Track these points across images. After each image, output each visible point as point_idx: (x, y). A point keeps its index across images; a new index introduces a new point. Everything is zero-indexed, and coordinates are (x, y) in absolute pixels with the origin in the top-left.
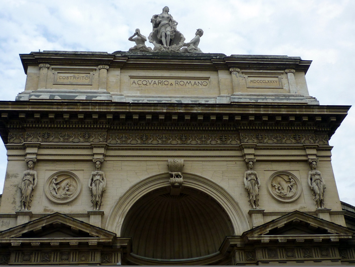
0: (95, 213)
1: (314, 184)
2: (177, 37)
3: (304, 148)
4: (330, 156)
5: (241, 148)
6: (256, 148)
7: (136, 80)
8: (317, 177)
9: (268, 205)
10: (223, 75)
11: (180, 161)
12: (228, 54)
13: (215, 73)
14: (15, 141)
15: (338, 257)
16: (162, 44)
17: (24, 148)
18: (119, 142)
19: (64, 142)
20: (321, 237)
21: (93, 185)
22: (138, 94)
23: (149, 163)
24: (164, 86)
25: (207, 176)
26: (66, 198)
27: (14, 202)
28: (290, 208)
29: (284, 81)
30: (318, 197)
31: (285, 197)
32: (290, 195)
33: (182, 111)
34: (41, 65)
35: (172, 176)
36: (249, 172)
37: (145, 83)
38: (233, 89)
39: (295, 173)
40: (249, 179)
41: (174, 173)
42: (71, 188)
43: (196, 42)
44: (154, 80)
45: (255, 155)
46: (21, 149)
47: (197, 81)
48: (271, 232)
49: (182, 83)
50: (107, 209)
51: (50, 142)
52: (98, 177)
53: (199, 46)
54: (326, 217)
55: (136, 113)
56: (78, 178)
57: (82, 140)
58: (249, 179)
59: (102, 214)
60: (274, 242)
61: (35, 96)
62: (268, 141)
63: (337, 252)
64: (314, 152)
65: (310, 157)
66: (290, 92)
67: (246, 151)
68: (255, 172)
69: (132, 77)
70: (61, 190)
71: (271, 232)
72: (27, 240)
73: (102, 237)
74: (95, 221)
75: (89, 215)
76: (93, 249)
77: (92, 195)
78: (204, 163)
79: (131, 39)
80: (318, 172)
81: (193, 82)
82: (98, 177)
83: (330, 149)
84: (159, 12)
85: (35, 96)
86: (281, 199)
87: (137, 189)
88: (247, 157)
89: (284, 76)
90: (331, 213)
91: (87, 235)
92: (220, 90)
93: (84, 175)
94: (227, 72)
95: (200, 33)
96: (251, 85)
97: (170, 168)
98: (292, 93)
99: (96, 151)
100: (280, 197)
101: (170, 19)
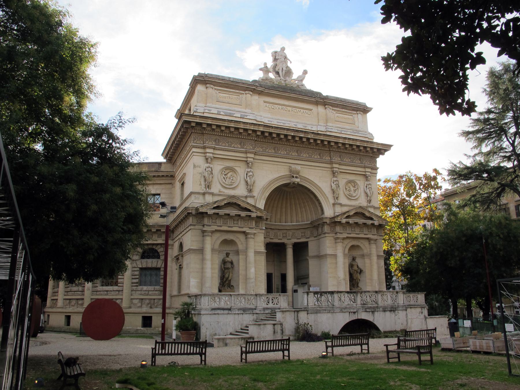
0: (251, 197)
1: (368, 190)
2: (289, 72)
3: (365, 167)
4: (376, 174)
5: (331, 163)
7: (268, 104)
8: (370, 186)
9: (343, 200)
10: (321, 109)
11: (298, 168)
12: (324, 94)
13: (316, 106)
14: (198, 142)
15: (376, 233)
16: (279, 76)
17: (204, 148)
18: (261, 150)
19: (228, 147)
20: (370, 222)
21: (248, 178)
23: (279, 167)
25: (311, 178)
26: (232, 185)
27: (200, 185)
29: (356, 119)
30: (369, 198)
31: (351, 196)
32: (354, 195)
33: (302, 136)
34: (208, 85)
35: (293, 177)
37: (273, 107)
38: (327, 122)
40: (335, 183)
41: (295, 175)
42: (234, 178)
43: (301, 79)
44: (278, 106)
45: (339, 169)
46: (201, 148)
47: (304, 111)
49: (295, 111)
50: (255, 194)
51: (220, 146)
53: (304, 82)
54: (372, 210)
55: (275, 133)
56: (238, 172)
57: (239, 146)
58: (335, 183)
59: (254, 197)
60: (348, 223)
61: (208, 110)
62: (347, 160)
63: (375, 230)
65: (367, 173)
66: (358, 128)
69: (265, 102)
70: (228, 179)
72: (216, 211)
73: (258, 213)
75: (246, 197)
76: (253, 219)
78: (310, 170)
79: (261, 69)
81: (302, 110)
83: (376, 169)
84: (279, 50)
85: (208, 110)
86: (349, 197)
87: (273, 183)
89: (356, 116)
90: (375, 208)
91: (249, 211)
92: (318, 120)
93: (241, 170)
94: (323, 107)
95: (305, 72)
99: (249, 155)
101: (286, 58)
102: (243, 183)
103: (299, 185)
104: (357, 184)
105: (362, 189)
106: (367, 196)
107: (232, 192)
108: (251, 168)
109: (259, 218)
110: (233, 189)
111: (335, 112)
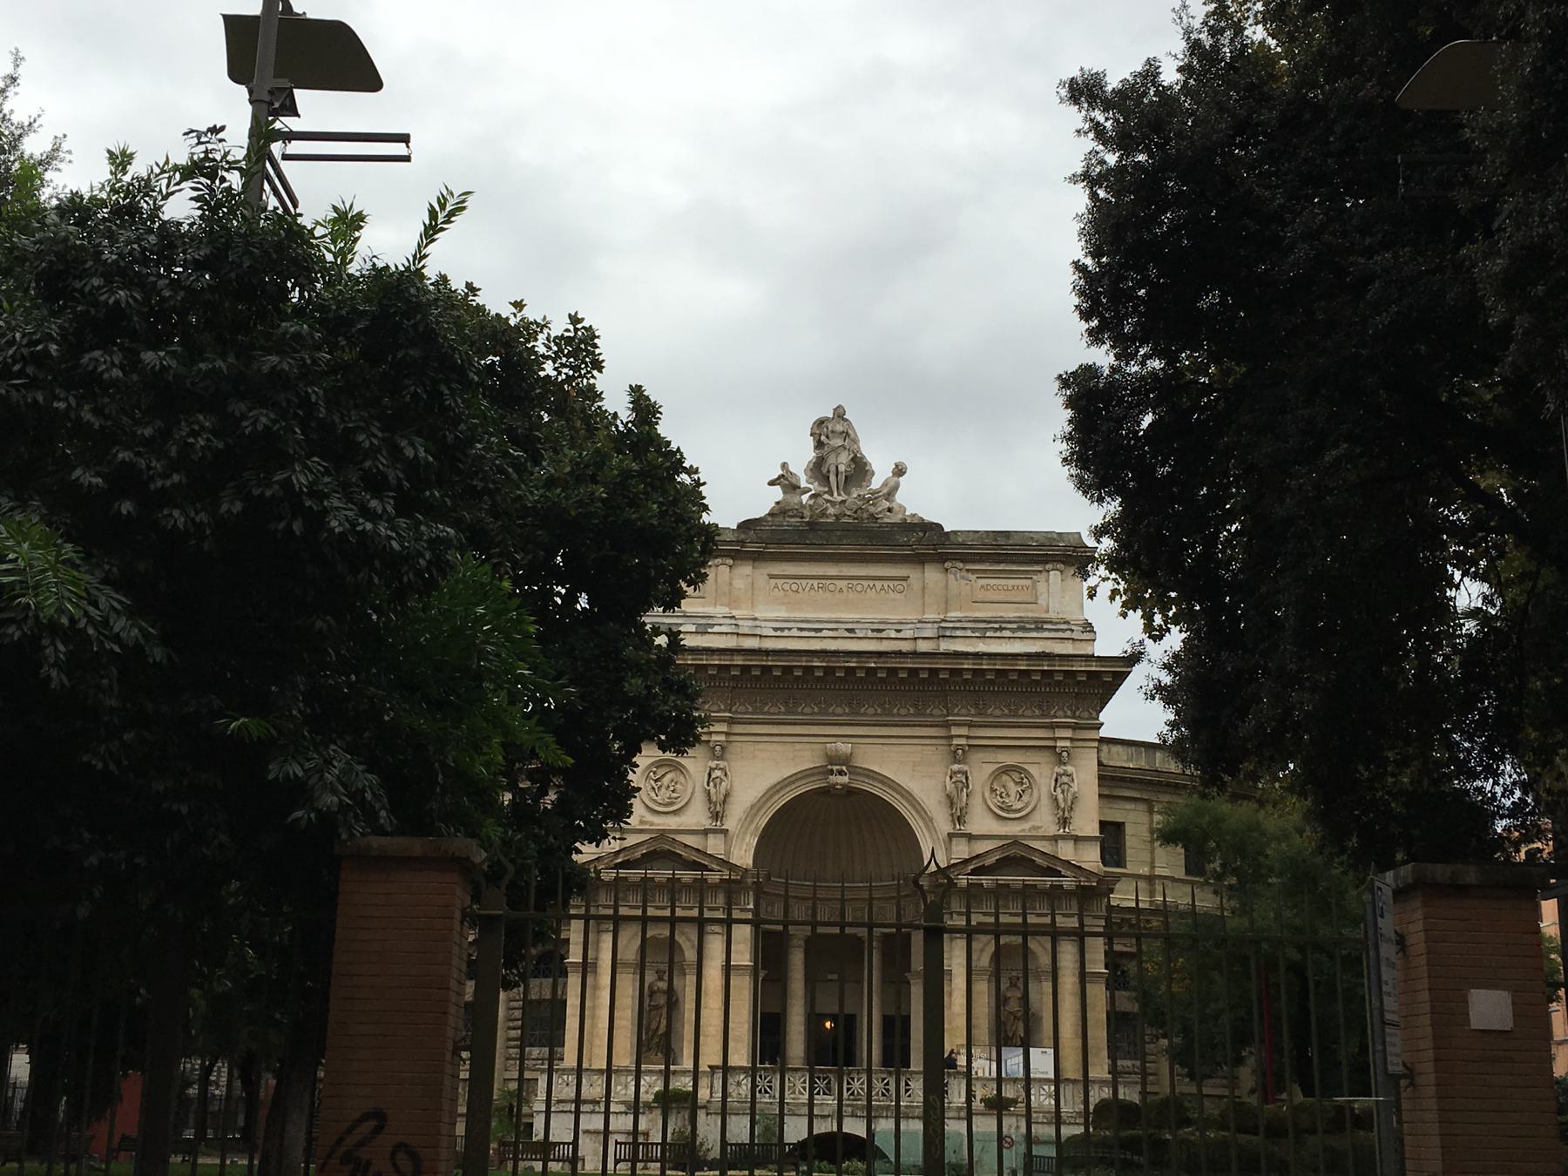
0: (715, 831)
3: (1052, 726)
6: (971, 725)
9: (980, 822)
11: (844, 747)
20: (1049, 881)
22: (784, 614)
23: (798, 746)
24: (828, 595)
26: (672, 804)
28: (1014, 829)
29: (1041, 586)
31: (1009, 809)
32: (1019, 805)
35: (831, 772)
36: (956, 767)
37: (794, 587)
39: (1032, 769)
43: (890, 494)
47: (886, 584)
48: (973, 873)
50: (730, 824)
52: (718, 773)
53: (900, 498)
64: (1068, 733)
65: (1059, 744)
67: (955, 731)
68: (965, 768)
69: (772, 577)
71: (973, 873)
74: (714, 846)
77: (710, 800)
80: (1069, 769)
81: (879, 584)
82: (718, 773)
86: (1003, 813)
88: (956, 741)
91: (706, 868)
95: (899, 471)
96: (980, 595)
97: (833, 759)
98: (1052, 615)
100: (1002, 809)
102: (699, 798)
103: (850, 792)
104: (1028, 775)
105: (1044, 790)
106: (1058, 807)
107: (671, 823)
108: (721, 758)
109: (733, 887)
110: (674, 812)
111: (973, 577)
